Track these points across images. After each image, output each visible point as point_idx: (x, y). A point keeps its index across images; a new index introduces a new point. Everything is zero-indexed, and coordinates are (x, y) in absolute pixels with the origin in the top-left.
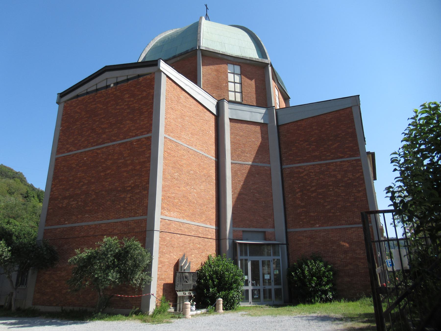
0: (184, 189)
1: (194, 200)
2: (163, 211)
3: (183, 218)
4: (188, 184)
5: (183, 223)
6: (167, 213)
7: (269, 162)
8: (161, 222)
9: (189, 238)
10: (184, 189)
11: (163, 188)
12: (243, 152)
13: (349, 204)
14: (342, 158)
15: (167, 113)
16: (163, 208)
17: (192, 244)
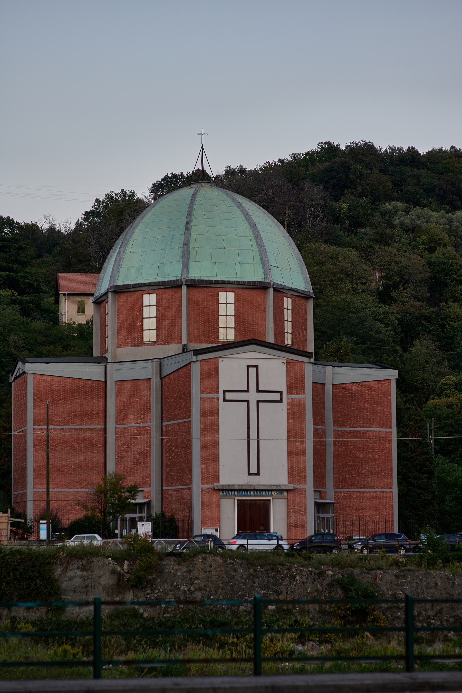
0: (59, 464)
1: (70, 472)
2: (35, 486)
3: (59, 488)
4: (62, 460)
5: (58, 492)
6: (39, 487)
7: (150, 421)
8: (33, 494)
9: (66, 502)
10: (59, 464)
11: (34, 469)
12: (127, 414)
13: (185, 466)
14: (185, 418)
15: (35, 407)
16: (34, 484)
17: (70, 506)
